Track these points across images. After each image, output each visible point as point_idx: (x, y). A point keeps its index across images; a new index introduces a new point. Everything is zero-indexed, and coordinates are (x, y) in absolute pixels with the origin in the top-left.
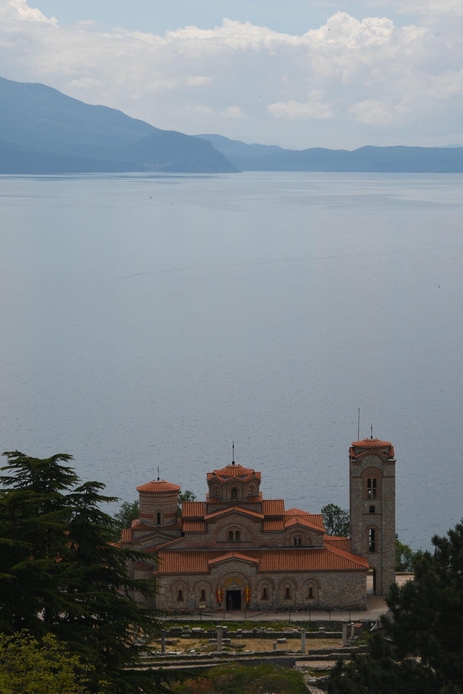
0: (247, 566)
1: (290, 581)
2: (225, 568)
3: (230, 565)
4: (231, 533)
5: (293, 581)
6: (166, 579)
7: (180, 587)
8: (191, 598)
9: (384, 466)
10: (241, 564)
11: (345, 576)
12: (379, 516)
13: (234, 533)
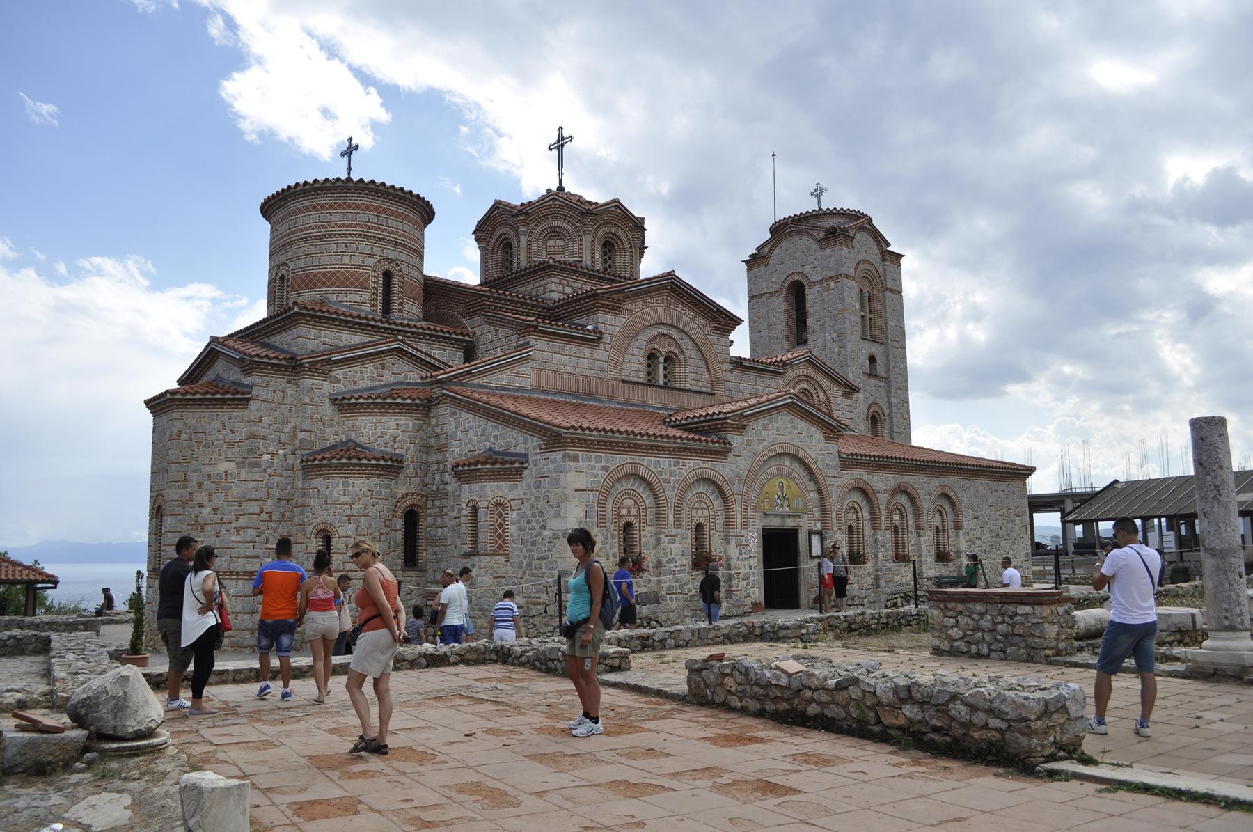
0: (818, 435)
1: (903, 500)
2: (763, 432)
3: (777, 425)
4: (652, 357)
5: (912, 500)
6: (585, 464)
7: (629, 508)
8: (669, 556)
9: (886, 263)
10: (803, 425)
11: (996, 491)
12: (883, 384)
13: (662, 360)
